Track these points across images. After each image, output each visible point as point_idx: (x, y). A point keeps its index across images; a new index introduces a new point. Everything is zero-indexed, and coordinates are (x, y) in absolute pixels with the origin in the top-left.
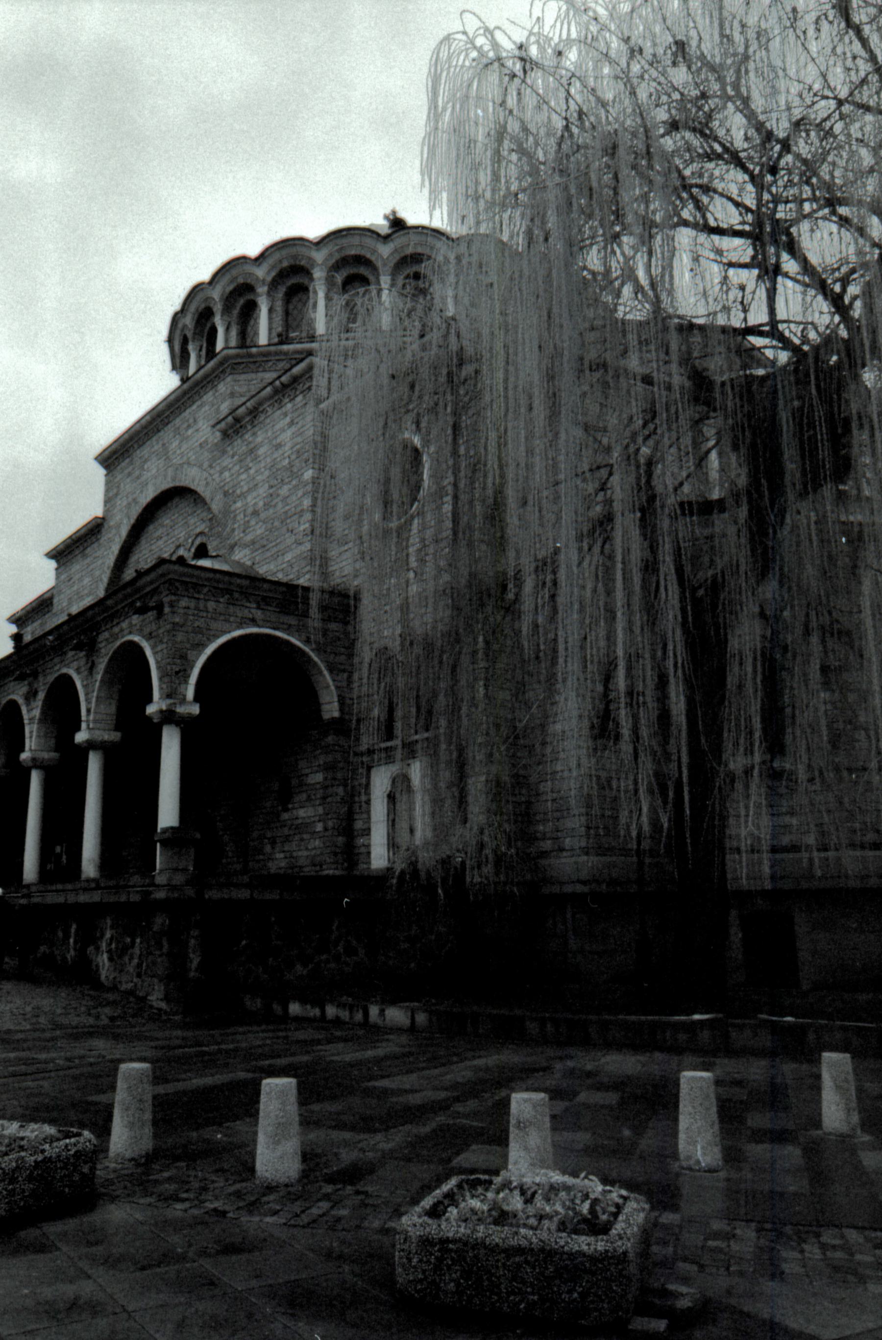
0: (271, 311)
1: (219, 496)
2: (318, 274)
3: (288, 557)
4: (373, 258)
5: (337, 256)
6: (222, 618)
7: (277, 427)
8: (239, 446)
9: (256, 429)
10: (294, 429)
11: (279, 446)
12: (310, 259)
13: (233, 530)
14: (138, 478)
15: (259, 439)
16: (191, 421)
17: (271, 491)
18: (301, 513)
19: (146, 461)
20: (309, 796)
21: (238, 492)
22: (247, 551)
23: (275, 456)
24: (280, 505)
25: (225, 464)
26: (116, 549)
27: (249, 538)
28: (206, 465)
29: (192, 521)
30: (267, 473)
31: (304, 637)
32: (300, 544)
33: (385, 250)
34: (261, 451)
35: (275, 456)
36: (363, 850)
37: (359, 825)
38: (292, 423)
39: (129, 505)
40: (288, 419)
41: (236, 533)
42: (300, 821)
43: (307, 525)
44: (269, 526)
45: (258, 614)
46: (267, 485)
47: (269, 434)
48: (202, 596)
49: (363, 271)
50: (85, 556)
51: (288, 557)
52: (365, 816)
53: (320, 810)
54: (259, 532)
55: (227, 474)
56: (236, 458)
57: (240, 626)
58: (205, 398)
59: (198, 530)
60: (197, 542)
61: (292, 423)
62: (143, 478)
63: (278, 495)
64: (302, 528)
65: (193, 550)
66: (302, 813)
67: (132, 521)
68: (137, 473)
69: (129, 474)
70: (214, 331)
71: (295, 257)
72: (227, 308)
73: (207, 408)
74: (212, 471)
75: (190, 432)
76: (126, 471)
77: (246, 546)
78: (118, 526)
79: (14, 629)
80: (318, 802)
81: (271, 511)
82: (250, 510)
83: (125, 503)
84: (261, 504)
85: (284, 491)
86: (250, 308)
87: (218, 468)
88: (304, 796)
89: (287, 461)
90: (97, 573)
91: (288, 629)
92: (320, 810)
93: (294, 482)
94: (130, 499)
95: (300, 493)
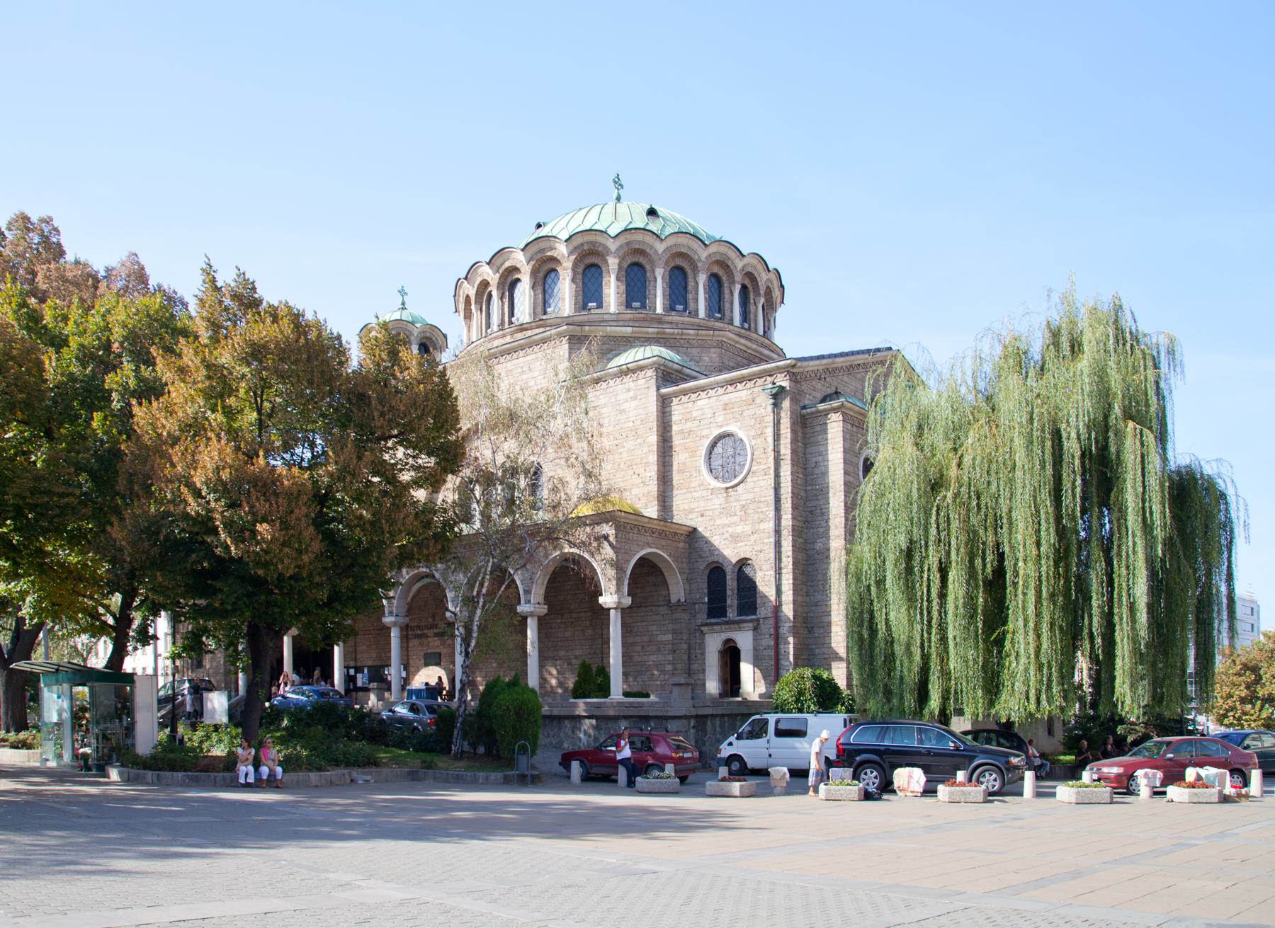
2: (613, 262)
4: (651, 252)
5: (626, 249)
11: (622, 412)
12: (606, 247)
16: (525, 369)
20: (659, 648)
33: (660, 247)
37: (695, 667)
38: (634, 398)
49: (642, 260)
64: (649, 474)
71: (593, 243)
80: (667, 652)
91: (662, 548)
95: (645, 450)
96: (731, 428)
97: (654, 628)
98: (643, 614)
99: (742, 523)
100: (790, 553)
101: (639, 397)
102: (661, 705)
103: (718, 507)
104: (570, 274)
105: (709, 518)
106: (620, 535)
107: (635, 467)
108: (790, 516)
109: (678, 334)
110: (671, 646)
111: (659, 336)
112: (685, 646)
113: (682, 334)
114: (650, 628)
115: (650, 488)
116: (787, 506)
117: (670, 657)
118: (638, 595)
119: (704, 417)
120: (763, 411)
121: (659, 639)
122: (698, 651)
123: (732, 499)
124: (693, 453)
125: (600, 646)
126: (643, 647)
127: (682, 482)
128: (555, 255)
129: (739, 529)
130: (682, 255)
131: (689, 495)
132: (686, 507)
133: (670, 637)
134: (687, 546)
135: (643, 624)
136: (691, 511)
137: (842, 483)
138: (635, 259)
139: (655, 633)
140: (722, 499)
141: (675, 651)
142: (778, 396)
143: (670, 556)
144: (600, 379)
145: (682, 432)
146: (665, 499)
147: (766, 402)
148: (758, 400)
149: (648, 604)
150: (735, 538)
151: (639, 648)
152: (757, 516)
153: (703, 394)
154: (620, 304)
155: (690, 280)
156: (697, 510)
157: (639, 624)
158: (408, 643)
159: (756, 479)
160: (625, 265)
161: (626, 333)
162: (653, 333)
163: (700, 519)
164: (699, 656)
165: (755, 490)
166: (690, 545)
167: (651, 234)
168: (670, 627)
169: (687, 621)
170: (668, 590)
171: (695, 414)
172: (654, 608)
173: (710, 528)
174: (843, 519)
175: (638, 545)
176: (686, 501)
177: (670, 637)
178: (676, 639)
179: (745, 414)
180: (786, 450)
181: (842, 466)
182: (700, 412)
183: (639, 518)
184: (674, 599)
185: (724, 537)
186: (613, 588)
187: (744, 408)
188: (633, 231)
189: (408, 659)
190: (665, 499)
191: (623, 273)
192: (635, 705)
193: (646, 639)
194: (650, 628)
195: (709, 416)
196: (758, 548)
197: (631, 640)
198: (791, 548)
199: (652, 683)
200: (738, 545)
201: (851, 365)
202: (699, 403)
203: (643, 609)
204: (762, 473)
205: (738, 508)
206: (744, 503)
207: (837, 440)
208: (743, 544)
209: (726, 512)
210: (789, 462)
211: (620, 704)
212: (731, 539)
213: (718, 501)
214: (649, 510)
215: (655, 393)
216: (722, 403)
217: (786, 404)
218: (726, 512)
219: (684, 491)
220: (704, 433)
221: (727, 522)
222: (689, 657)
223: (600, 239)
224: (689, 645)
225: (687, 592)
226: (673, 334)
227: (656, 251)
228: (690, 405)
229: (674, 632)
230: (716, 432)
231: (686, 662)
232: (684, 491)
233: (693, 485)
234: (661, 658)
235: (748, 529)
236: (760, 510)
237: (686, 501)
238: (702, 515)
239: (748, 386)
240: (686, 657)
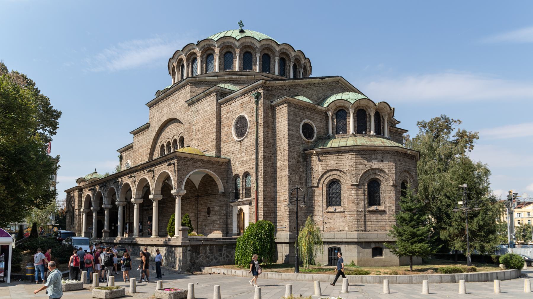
0: (202, 62)
1: (187, 123)
3: (209, 145)
6: (191, 166)
7: (205, 105)
8: (193, 108)
9: (198, 105)
10: (210, 107)
11: (205, 111)
13: (192, 134)
14: (161, 113)
15: (200, 108)
16: (178, 98)
17: (203, 125)
19: (163, 108)
20: (216, 213)
21: (193, 123)
22: (196, 141)
23: (205, 114)
24: (206, 130)
25: (189, 114)
26: (154, 134)
27: (197, 137)
28: (183, 113)
29: (178, 129)
30: (202, 119)
31: (214, 171)
34: (200, 112)
35: (205, 114)
36: (231, 228)
37: (229, 221)
38: (209, 105)
39: (158, 121)
40: (208, 104)
41: (193, 135)
42: (213, 220)
43: (215, 137)
44: (203, 135)
45: (201, 165)
46: (202, 123)
47: (203, 107)
48: (186, 161)
49: (231, 50)
50: (144, 135)
51: (209, 145)
52: (231, 219)
53: (219, 217)
54: (200, 136)
55: (189, 117)
56: (192, 112)
57: (196, 168)
58: (182, 91)
59: (181, 132)
60: (181, 135)
61: (209, 105)
62: (162, 113)
63: (206, 126)
64: (213, 137)
65: (179, 137)
66: (213, 218)
67: (159, 126)
68: (160, 111)
69: (158, 111)
70: (183, 66)
72: (188, 60)
73: (183, 95)
74: (185, 115)
75: (177, 101)
76: (157, 110)
77: (196, 140)
78: (155, 127)
79: (119, 154)
80: (218, 215)
81: (204, 131)
82: (197, 129)
83: (157, 120)
84: (200, 128)
85: (208, 125)
86: (195, 59)
87: (187, 115)
88: (214, 213)
89: (208, 116)
90: (148, 141)
91: (210, 169)
92: (219, 217)
93: (210, 123)
94: (158, 119)
95: (212, 127)
96: (243, 114)
99: (246, 156)
100: (262, 169)
101: (211, 105)
103: (237, 149)
104: (200, 58)
105: (234, 155)
107: (209, 135)
108: (262, 151)
109: (238, 78)
111: (230, 80)
112: (225, 212)
113: (240, 78)
116: (261, 147)
119: (234, 110)
120: (253, 105)
122: (231, 214)
123: (243, 145)
124: (230, 126)
125: (197, 213)
128: (194, 51)
129: (245, 159)
130: (249, 46)
131: (228, 145)
132: (227, 150)
135: (211, 202)
136: (229, 152)
137: (287, 135)
138: (227, 50)
140: (239, 146)
142: (257, 97)
143: (215, 172)
144: (199, 99)
145: (226, 118)
146: (218, 148)
147: (253, 100)
148: (252, 100)
150: (243, 163)
152: (251, 153)
153: (234, 101)
154: (220, 68)
155: (253, 56)
156: (231, 151)
158: (143, 213)
159: (250, 136)
160: (223, 53)
161: (215, 79)
162: (227, 79)
163: (232, 155)
164: (231, 216)
165: (251, 141)
167: (233, 38)
171: (231, 110)
172: (214, 196)
173: (235, 159)
174: (288, 152)
176: (227, 148)
179: (247, 107)
180: (261, 121)
181: (287, 127)
182: (232, 108)
185: (239, 162)
187: (247, 105)
188: (225, 38)
189: (143, 219)
190: (218, 148)
191: (223, 56)
195: (235, 110)
196: (251, 167)
198: (262, 166)
200: (244, 166)
201: (309, 84)
202: (232, 104)
204: (253, 133)
205: (244, 150)
206: (246, 147)
207: (285, 115)
208: (246, 165)
209: (241, 152)
210: (262, 127)
212: (242, 163)
213: (238, 147)
215: (216, 102)
216: (240, 103)
217: (261, 101)
218: (241, 152)
219: (227, 143)
220: (234, 117)
221: (241, 156)
222: (227, 217)
223: (211, 43)
226: (236, 78)
227: (236, 45)
228: (229, 105)
230: (237, 116)
233: (230, 140)
234: (216, 217)
235: (248, 158)
236: (252, 149)
237: (227, 148)
238: (232, 154)
239: (248, 95)
240: (225, 217)
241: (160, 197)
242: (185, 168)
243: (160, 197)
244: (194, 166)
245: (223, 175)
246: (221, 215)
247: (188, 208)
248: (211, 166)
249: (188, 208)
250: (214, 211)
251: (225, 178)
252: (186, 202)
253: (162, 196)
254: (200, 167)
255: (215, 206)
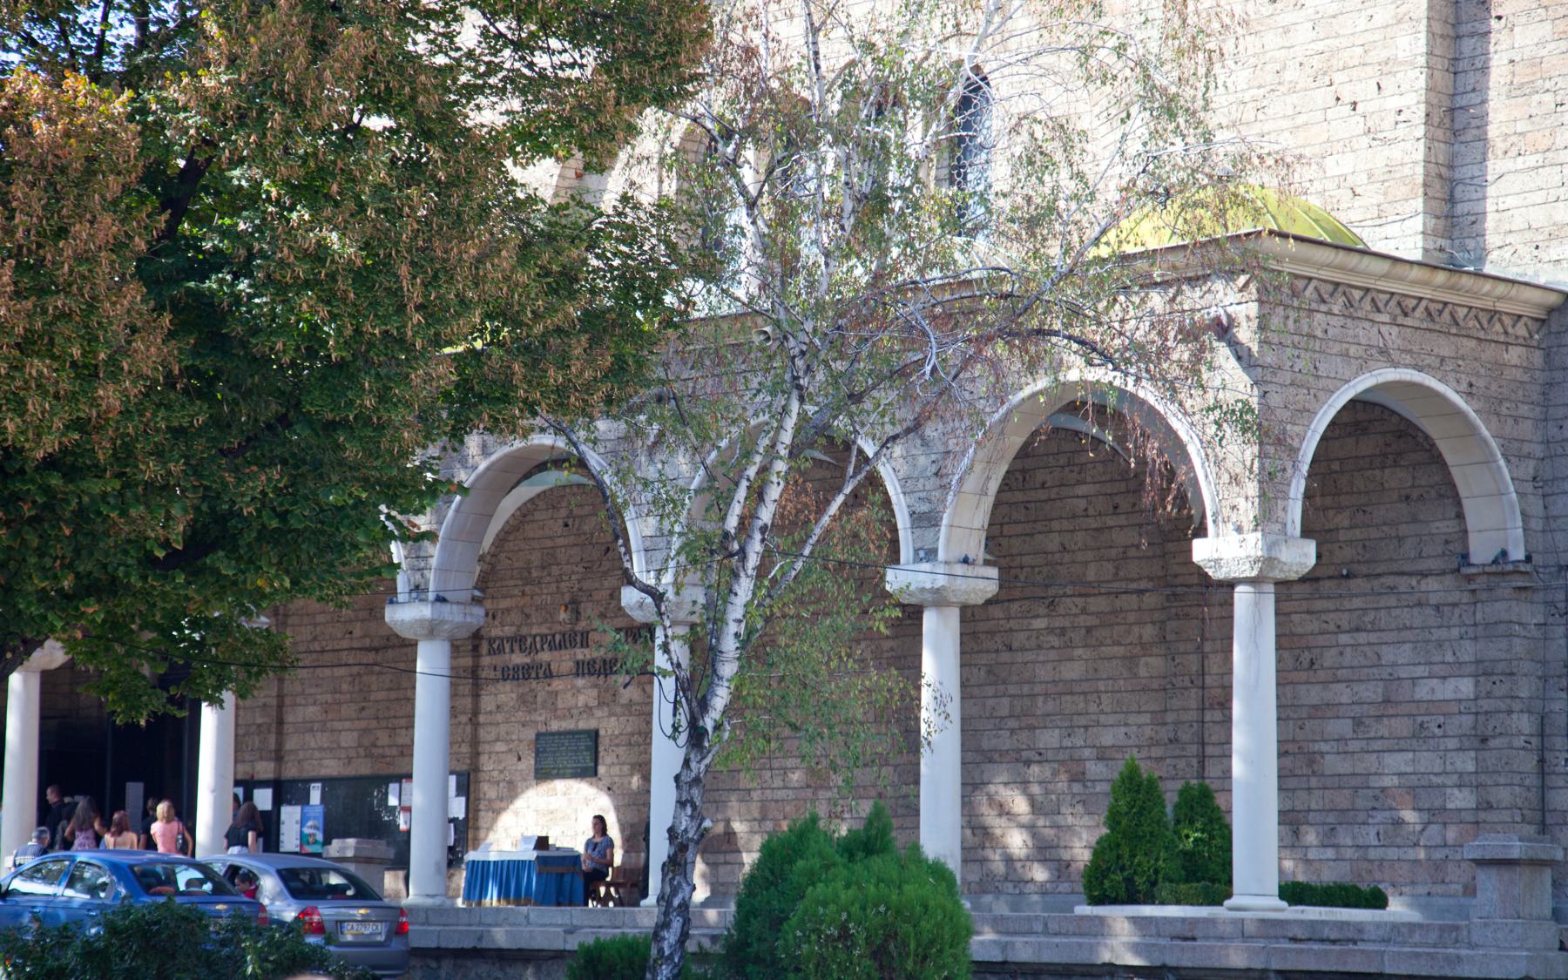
6: (1336, 348)
18: (1388, 66)
31: (1464, 387)
32: (1386, 142)
45: (1393, 335)
57: (1363, 367)
64: (1395, 103)
80: (1452, 743)
91: (1439, 366)
97: (1405, 653)
98: (1357, 603)
102: (1433, 937)
106: (1275, 322)
110: (1468, 721)
112: (1524, 724)
114: (1388, 655)
115: (1396, 153)
117: (1466, 762)
118: (1342, 536)
121: (1422, 692)
126: (1358, 722)
127: (1521, 127)
132: (1538, 217)
133: (1466, 687)
134: (1538, 358)
135: (1362, 638)
139: (1403, 673)
141: (1484, 740)
143: (1469, 395)
149: (1381, 568)
151: (1344, 727)
157: (1344, 639)
166: (1548, 356)
168: (1468, 651)
169: (1536, 633)
170: (1460, 516)
172: (1403, 583)
175: (1345, 355)
176: (1539, 197)
177: (1466, 687)
178: (1489, 695)
183: (1354, 260)
184: (1481, 551)
186: (1247, 511)
192: (1326, 933)
193: (1371, 692)
194: (1388, 655)
197: (1312, 695)
199: (1392, 853)
203: (1358, 584)
211: (1270, 928)
214: (1390, 230)
219: (1531, 160)
222: (1542, 761)
224: (1543, 720)
225: (1536, 524)
229: (1483, 671)
231: (1533, 780)
232: (1531, 160)
234: (1428, 761)
237: (1539, 197)
240: (1529, 763)
241: (983, 583)
242: (1299, 365)
243: (983, 583)
244: (1353, 350)
245: (1516, 420)
246: (1493, 743)
247: (1072, 671)
248: (1445, 347)
249: (1072, 671)
250: (1404, 709)
251: (1526, 448)
252: (1040, 624)
253: (993, 572)
254: (1385, 355)
255: (1420, 671)
